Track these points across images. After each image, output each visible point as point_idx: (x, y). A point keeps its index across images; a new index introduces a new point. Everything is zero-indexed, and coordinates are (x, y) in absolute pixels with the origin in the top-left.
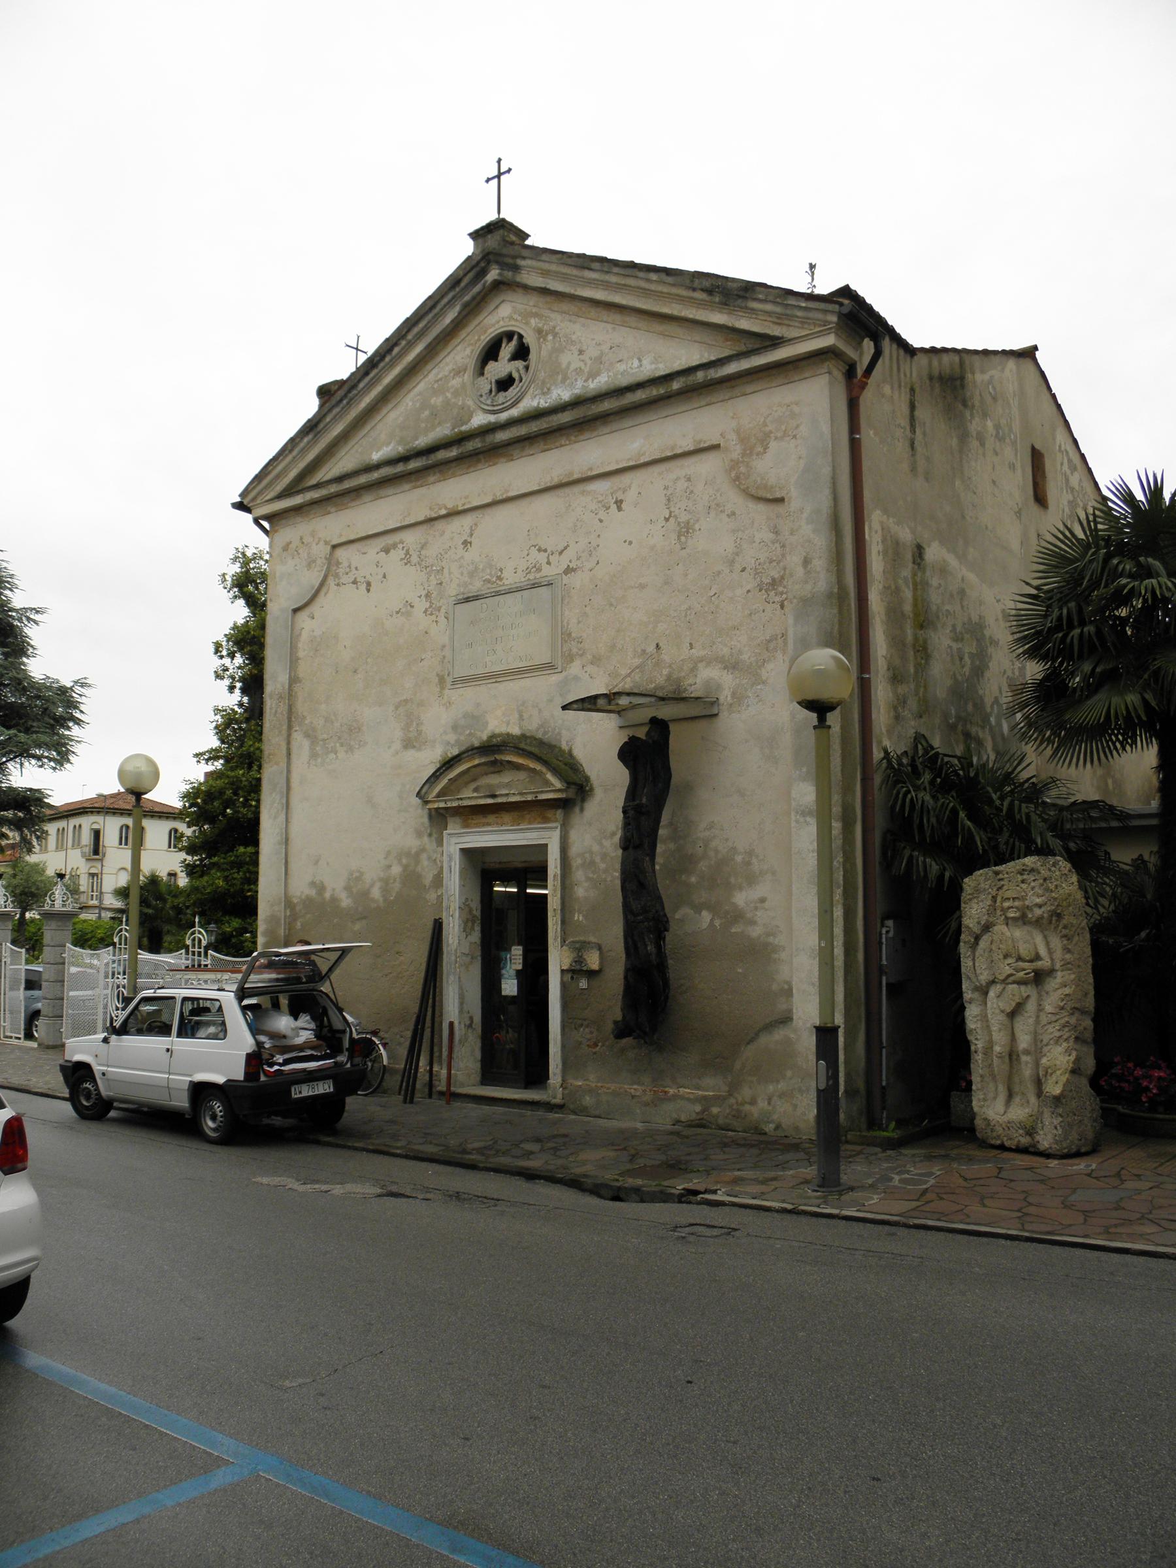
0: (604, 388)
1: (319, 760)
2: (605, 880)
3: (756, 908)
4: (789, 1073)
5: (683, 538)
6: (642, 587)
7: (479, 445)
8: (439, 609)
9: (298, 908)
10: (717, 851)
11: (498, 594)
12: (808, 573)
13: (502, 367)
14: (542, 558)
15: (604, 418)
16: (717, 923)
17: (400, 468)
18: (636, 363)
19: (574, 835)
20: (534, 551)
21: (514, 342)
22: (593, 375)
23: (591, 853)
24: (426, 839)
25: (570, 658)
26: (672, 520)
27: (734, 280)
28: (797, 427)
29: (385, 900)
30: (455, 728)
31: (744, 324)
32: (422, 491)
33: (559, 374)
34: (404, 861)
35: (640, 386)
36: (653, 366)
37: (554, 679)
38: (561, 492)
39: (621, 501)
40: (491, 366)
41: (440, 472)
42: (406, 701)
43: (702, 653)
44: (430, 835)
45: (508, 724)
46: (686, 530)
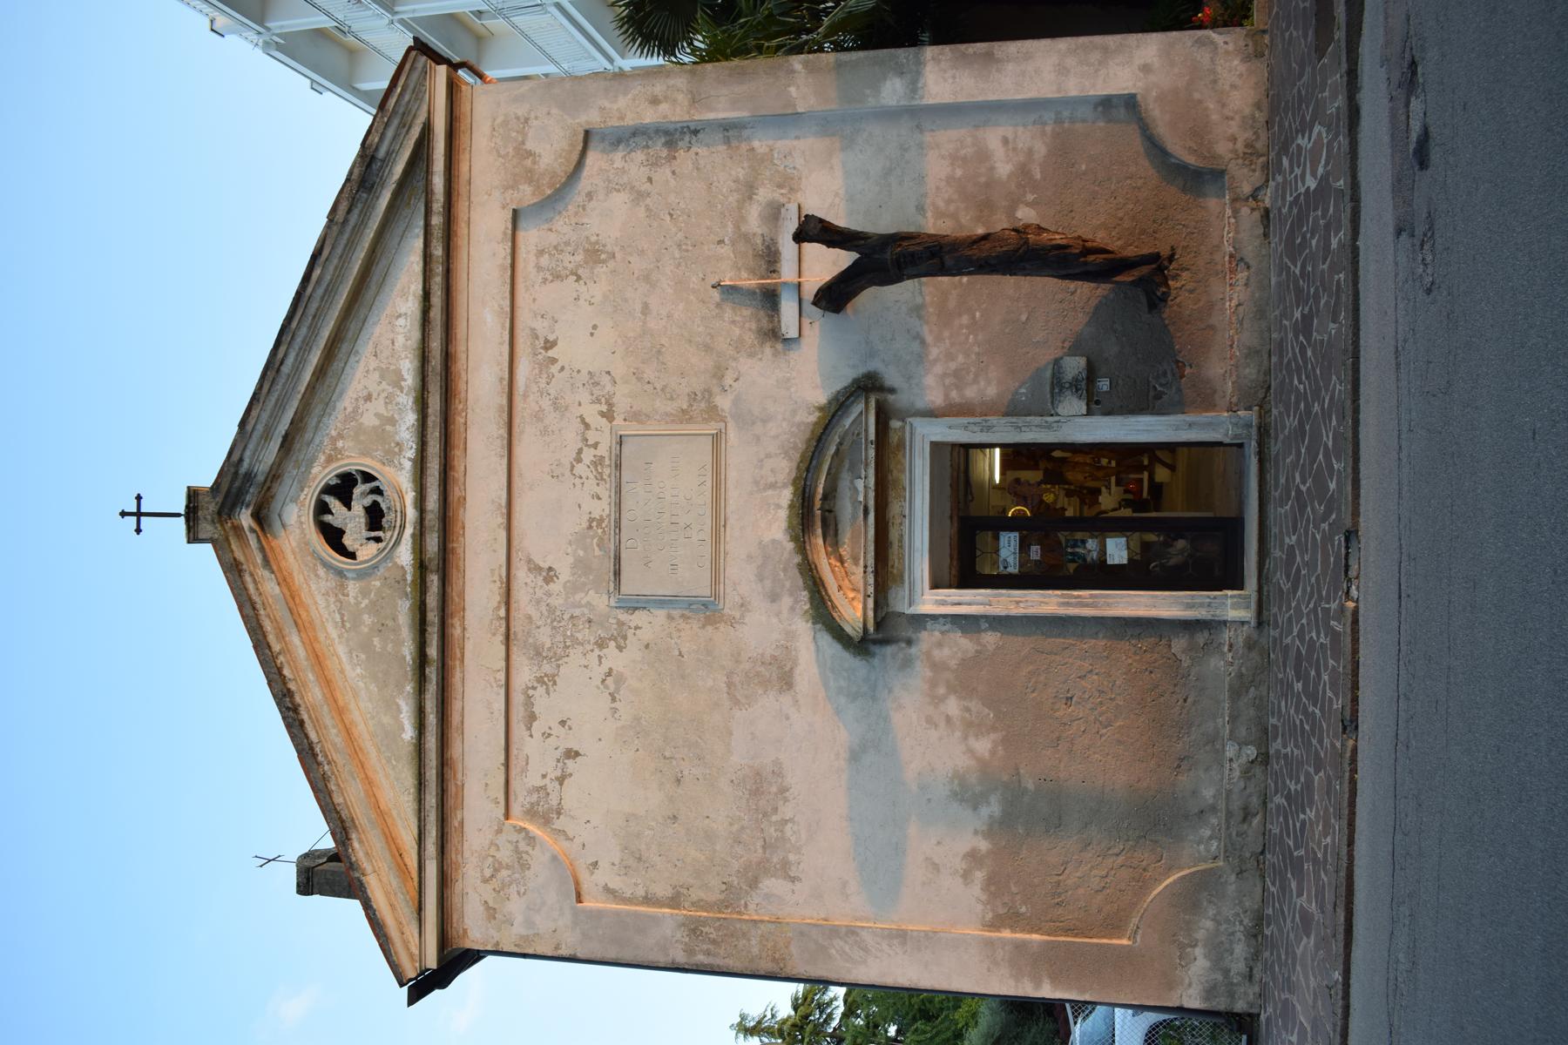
0: (416, 363)
1: (791, 857)
2: (978, 354)
3: (1014, 149)
4: (1197, 96)
5: (603, 256)
6: (646, 309)
8: (621, 624)
9: (1002, 911)
10: (949, 201)
11: (618, 525)
12: (666, 98)
13: (351, 520)
14: (588, 455)
15: (448, 357)
16: (1030, 197)
17: (432, 673)
18: (401, 321)
19: (920, 404)
20: (580, 469)
22: (397, 381)
23: (945, 375)
24: (913, 650)
25: (713, 412)
26: (580, 272)
27: (351, 173)
28: (518, 118)
29: (994, 729)
30: (774, 598)
31: (399, 169)
33: (382, 435)
34: (942, 691)
35: (426, 295)
37: (733, 435)
38: (516, 430)
39: (546, 341)
40: (347, 541)
42: (730, 685)
43: (730, 228)
44: (909, 642)
45: (778, 506)
46: (595, 254)
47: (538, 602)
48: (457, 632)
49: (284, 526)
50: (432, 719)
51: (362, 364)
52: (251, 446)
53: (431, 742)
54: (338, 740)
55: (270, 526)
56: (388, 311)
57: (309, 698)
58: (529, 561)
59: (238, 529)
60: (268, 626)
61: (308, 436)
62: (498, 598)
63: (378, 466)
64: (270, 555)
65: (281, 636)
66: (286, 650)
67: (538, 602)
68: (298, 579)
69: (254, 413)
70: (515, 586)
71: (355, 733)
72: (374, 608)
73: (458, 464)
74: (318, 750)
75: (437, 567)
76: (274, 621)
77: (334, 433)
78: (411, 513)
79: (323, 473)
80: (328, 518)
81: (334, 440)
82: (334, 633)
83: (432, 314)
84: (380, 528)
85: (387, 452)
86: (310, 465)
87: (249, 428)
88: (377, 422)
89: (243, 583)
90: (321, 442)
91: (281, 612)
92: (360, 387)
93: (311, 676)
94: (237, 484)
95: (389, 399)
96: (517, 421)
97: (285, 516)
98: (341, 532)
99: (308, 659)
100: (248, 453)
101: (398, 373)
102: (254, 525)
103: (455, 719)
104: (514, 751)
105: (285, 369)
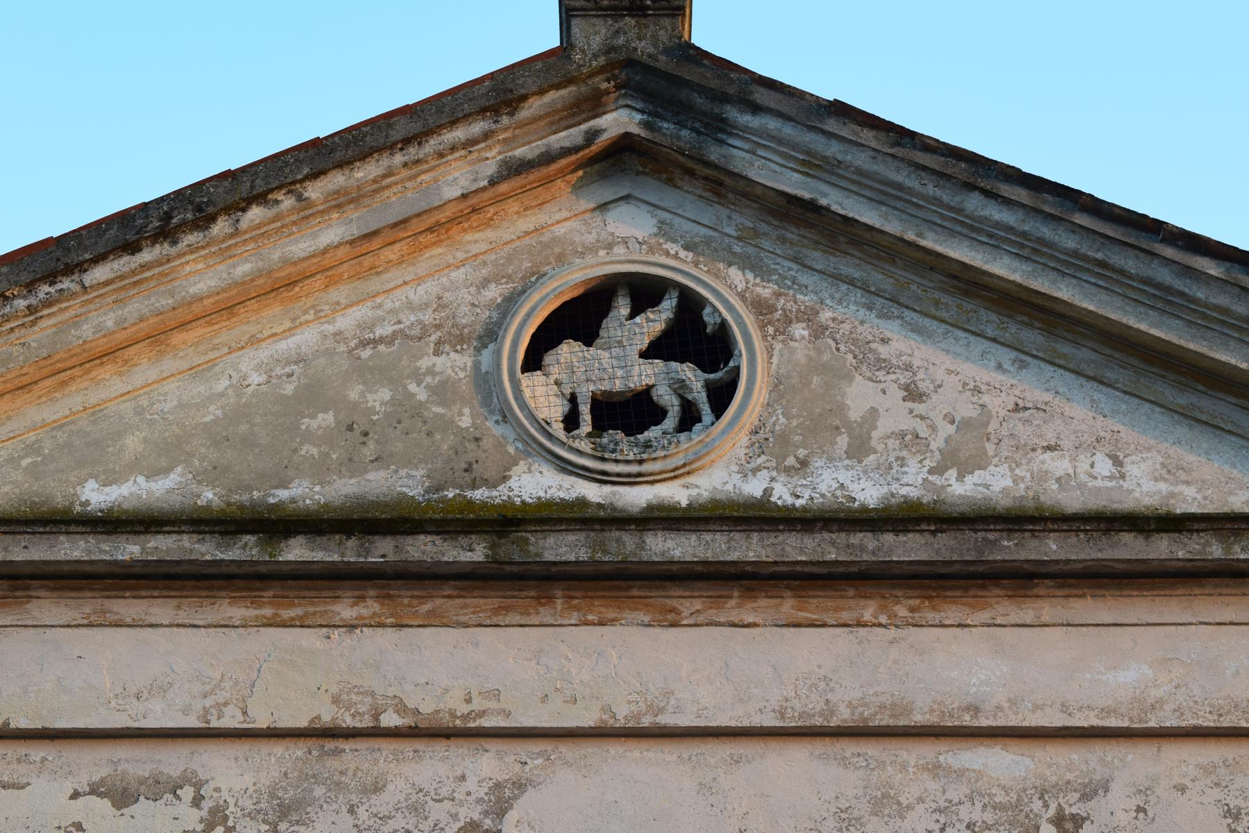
0: (1004, 503)
7: (583, 555)
13: (621, 357)
15: (1023, 579)
17: (245, 549)
18: (1104, 466)
21: (666, 311)
22: (958, 460)
32: (308, 639)
33: (821, 425)
36: (1163, 487)
38: (849, 748)
40: (568, 352)
41: (383, 598)
47: (416, 809)
48: (345, 610)
49: (603, 207)
50: (129, 550)
51: (997, 378)
52: (788, 130)
53: (72, 549)
54: (87, 331)
55: (603, 176)
56: (1128, 435)
57: (192, 265)
58: (520, 786)
59: (594, 105)
60: (366, 172)
61: (817, 258)
62: (426, 708)
63: (750, 418)
64: (534, 176)
65: (340, 202)
66: (307, 213)
67: (416, 809)
68: (477, 240)
69: (867, 136)
70: (458, 751)
71: (105, 372)
72: (406, 413)
73: (758, 609)
74: (66, 284)
75: (511, 563)
76: (379, 185)
77: (825, 316)
78: (637, 497)
79: (728, 291)
80: (622, 307)
81: (808, 316)
82: (346, 321)
83: (1127, 537)
84: (600, 426)
85: (784, 440)
86: (746, 263)
87: (832, 125)
88: (854, 415)
89: (467, 117)
90: (803, 288)
91: (398, 201)
92: (940, 375)
93: (243, 269)
94: (699, 101)
95: (912, 441)
96: (872, 749)
97: (623, 209)
98: (589, 338)
99: (286, 262)
100: (772, 124)
101: (977, 462)
102: (604, 139)
103: (127, 608)
104: (38, 752)
105: (974, 203)
